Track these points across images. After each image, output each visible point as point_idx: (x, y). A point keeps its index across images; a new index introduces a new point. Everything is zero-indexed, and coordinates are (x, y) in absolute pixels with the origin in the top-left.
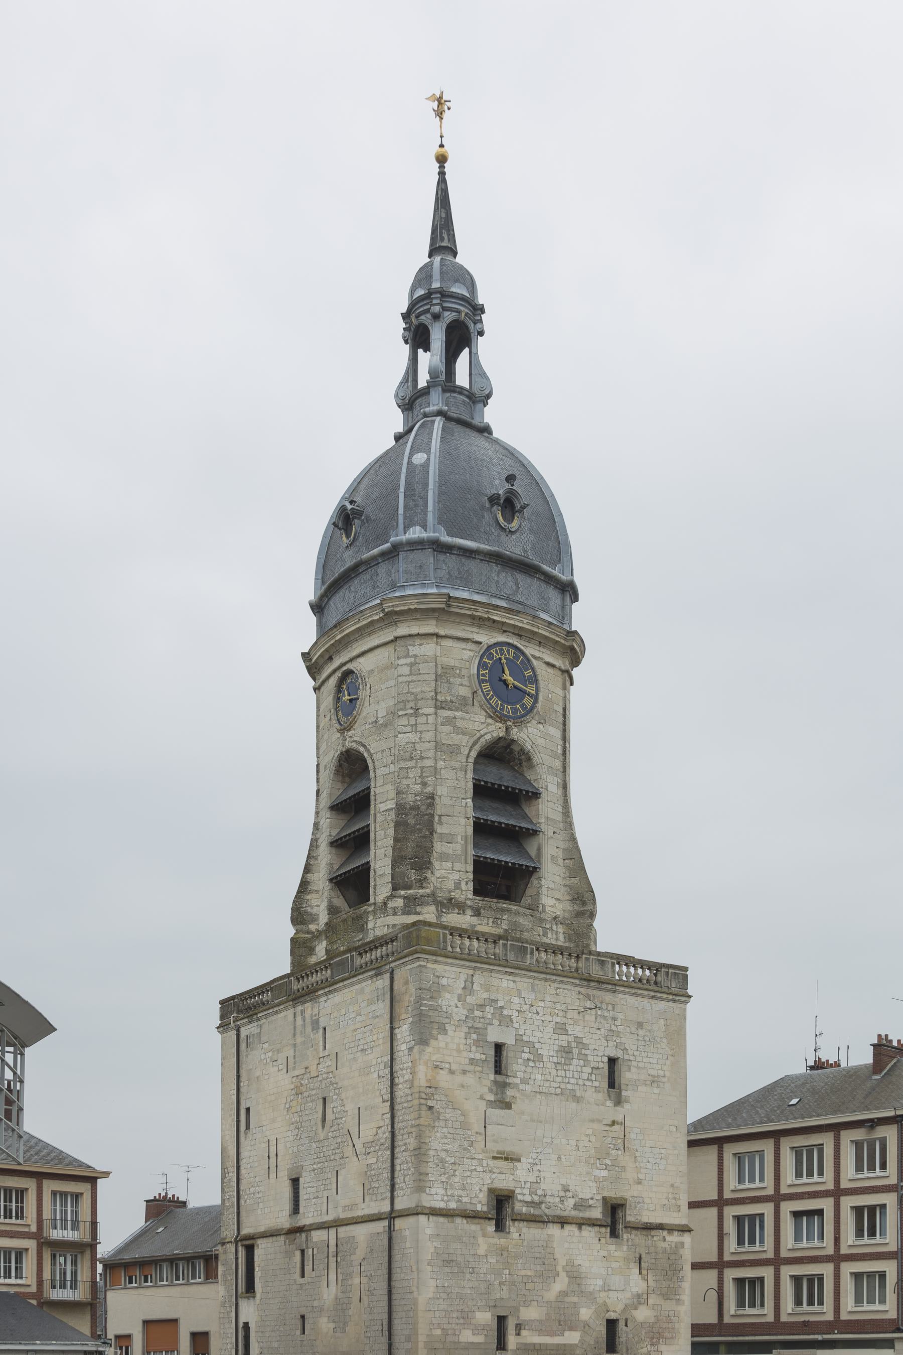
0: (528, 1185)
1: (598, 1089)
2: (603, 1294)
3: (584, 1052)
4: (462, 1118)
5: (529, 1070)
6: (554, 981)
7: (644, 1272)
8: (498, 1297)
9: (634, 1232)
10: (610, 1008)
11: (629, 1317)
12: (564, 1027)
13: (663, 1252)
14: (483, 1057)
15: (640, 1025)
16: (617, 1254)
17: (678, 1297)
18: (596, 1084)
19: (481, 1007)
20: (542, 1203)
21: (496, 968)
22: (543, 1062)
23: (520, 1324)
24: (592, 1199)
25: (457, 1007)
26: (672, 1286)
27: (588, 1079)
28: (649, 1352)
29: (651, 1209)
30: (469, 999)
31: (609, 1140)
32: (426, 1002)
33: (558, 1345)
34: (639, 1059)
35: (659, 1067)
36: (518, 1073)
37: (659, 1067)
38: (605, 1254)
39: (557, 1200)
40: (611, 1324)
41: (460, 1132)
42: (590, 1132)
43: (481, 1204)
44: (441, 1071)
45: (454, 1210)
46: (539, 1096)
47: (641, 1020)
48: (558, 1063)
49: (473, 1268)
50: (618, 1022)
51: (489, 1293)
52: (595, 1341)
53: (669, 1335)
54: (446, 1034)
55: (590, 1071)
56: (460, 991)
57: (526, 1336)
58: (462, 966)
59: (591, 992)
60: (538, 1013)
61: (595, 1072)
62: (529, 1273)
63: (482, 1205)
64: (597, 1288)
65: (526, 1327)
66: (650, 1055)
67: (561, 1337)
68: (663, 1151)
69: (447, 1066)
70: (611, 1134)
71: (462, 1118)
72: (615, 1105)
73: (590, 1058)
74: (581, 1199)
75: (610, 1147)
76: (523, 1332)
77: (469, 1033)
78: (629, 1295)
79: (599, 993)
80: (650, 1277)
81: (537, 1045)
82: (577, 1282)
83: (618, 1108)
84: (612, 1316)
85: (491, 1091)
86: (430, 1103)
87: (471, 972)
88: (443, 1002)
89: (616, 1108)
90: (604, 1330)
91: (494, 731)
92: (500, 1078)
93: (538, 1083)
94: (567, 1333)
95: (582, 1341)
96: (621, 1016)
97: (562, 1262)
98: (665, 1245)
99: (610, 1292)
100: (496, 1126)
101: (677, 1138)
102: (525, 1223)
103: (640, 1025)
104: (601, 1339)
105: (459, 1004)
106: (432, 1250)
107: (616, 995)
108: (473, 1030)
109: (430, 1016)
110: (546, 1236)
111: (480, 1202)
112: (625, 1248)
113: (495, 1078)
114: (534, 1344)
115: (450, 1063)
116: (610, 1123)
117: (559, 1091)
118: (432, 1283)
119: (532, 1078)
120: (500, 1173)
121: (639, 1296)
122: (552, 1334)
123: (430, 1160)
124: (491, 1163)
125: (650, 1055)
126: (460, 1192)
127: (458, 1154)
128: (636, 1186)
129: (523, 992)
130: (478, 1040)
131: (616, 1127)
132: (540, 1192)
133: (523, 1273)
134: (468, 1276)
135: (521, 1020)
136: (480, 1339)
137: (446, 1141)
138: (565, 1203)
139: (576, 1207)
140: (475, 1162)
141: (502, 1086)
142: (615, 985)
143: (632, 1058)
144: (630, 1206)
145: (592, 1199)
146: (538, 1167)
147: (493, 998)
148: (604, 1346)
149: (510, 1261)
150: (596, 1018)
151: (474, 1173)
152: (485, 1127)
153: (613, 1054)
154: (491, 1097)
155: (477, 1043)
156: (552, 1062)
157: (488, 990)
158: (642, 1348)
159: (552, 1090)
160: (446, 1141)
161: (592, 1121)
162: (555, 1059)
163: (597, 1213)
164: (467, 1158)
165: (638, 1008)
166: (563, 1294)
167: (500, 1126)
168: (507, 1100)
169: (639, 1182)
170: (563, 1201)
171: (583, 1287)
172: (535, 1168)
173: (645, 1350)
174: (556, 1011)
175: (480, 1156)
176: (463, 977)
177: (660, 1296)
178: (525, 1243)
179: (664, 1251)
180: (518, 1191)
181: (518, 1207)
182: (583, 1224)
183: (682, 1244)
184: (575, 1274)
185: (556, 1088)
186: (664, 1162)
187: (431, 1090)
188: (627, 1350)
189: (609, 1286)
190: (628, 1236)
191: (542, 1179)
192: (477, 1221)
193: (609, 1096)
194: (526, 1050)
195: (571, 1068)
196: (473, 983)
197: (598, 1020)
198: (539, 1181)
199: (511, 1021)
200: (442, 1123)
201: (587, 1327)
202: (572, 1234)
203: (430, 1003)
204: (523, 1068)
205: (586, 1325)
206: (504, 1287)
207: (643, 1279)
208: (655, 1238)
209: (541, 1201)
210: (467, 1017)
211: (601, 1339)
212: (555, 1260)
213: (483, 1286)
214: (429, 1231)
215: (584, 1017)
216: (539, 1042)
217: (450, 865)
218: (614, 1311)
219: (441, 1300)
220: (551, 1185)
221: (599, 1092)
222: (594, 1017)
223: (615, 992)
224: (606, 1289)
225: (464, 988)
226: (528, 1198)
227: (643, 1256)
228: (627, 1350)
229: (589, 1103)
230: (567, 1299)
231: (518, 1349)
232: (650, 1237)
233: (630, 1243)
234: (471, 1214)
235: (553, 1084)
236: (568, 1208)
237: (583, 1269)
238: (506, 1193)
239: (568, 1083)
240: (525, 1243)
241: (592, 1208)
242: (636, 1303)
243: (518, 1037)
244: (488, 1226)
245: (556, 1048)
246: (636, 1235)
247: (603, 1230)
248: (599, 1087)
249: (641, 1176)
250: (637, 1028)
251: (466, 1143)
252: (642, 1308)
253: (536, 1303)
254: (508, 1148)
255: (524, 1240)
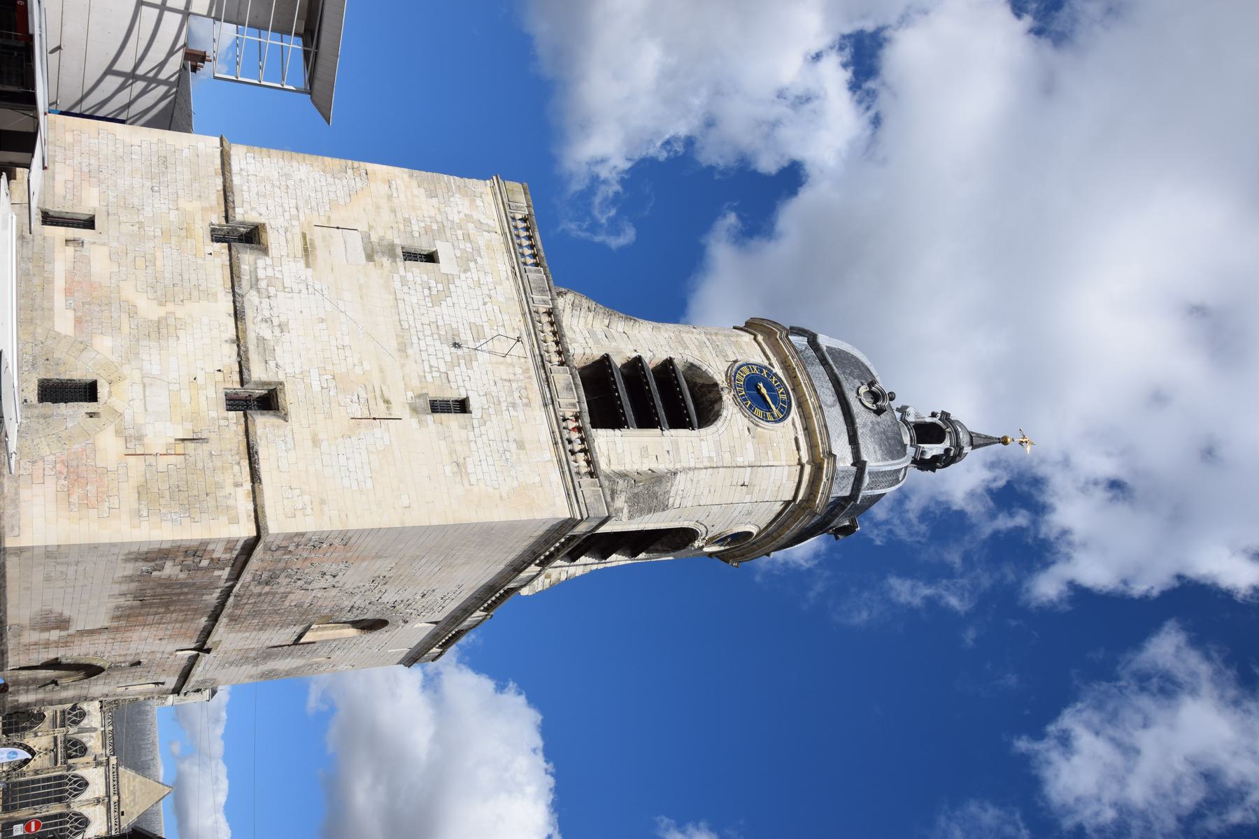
0: (278, 275)
1: (424, 379)
2: (136, 375)
3: (462, 362)
4: (341, 202)
5: (419, 288)
6: (526, 325)
7: (180, 448)
8: (121, 219)
9: (241, 429)
10: (525, 400)
11: (103, 419)
12: (481, 336)
13: (216, 483)
14: (416, 235)
15: (521, 445)
16: (202, 399)
17: (145, 513)
18: (429, 377)
19: (467, 238)
20: (259, 292)
21: (513, 254)
22: (433, 306)
23: (82, 246)
24: (277, 366)
25: (459, 212)
26: (162, 501)
27: (431, 367)
28: (43, 459)
29: (280, 463)
30: (471, 226)
31: (363, 395)
32: (452, 181)
33: (51, 299)
34: (479, 440)
35: (480, 476)
36: (410, 274)
37: (480, 476)
38: (200, 381)
39: (267, 314)
40: (89, 392)
41: (326, 200)
42: (367, 366)
43: (245, 214)
44: (387, 186)
45: (231, 181)
46: (391, 297)
47: (527, 447)
48: (437, 326)
49: (159, 191)
50: (513, 413)
51: (126, 208)
52: (60, 359)
53: (74, 499)
54: (427, 197)
55: (443, 369)
56: (475, 217)
57: (65, 251)
58: (501, 221)
59: (532, 372)
60: (485, 304)
61: (443, 375)
62: (159, 263)
63: (243, 215)
64: (147, 366)
65: (79, 253)
66: (490, 459)
67: (63, 305)
68: (369, 484)
69: (395, 194)
70: (371, 396)
71: (343, 203)
72: (410, 405)
73: (457, 369)
74: (274, 350)
75: (353, 395)
76: (70, 250)
77: (437, 222)
78: (140, 420)
79: (536, 386)
80: (173, 459)
81: (448, 299)
82: (153, 335)
83: (408, 410)
84: (102, 391)
85: (382, 239)
86: (350, 171)
87: (499, 231)
88: (457, 198)
89: (407, 406)
90: (79, 372)
91: (720, 379)
92: (399, 252)
93: (406, 297)
94: (70, 315)
95: (58, 337)
96: (522, 417)
97: (180, 312)
98: (229, 489)
99: (141, 386)
100: (343, 242)
101: (394, 508)
102: (228, 263)
103: (521, 445)
104: (62, 369)
105: (462, 215)
106: (178, 147)
107: (543, 409)
108: (440, 225)
109: (440, 183)
110: (214, 290)
111: (246, 212)
112: (213, 414)
113: (397, 245)
114: (52, 262)
115: (398, 197)
116: (386, 395)
117: (405, 325)
118: (136, 141)
119: (412, 292)
120: (287, 240)
121: (140, 438)
122: (69, 292)
123: (286, 162)
124: (297, 231)
125: (491, 462)
126: (254, 190)
127: (299, 193)
128: (310, 438)
129: (501, 287)
130: (432, 230)
131: (383, 406)
132: (272, 290)
133: (159, 254)
134: (148, 184)
135: (470, 281)
136: (59, 189)
137: (312, 182)
138: (264, 325)
139: (261, 340)
140: (294, 211)
141: (390, 251)
142: (553, 403)
143: (477, 431)
144: (278, 427)
145: (277, 366)
146: (304, 291)
147: (482, 253)
148: (53, 375)
149: (174, 240)
150: (506, 380)
151: (281, 209)
152: (338, 228)
153: (473, 404)
154: (374, 238)
155: (427, 230)
156: (437, 318)
157: (488, 247)
158: (48, 445)
159: (403, 317)
160: (312, 182)
161: (382, 371)
162: (440, 323)
163: (258, 372)
164: (297, 203)
165: (539, 441)
166: (132, 312)
167: (344, 246)
168: (376, 258)
169: (316, 442)
170: (266, 322)
171: (146, 343)
172: (303, 287)
173: (45, 451)
174: (495, 328)
175: (302, 218)
176: (491, 222)
177: (143, 479)
178: (200, 261)
179: (219, 486)
180: (268, 260)
181: (247, 258)
182: (238, 346)
183: (234, 520)
184: (164, 331)
185: (408, 321)
186: (355, 487)
187: (364, 174)
188: (45, 417)
189: (151, 384)
190: (231, 419)
191: (290, 295)
192: (222, 202)
193: (419, 396)
194: (440, 287)
195: (438, 343)
196: (489, 232)
197: (507, 384)
198: (286, 290)
199: (467, 270)
200: (330, 180)
201: (82, 347)
202: (222, 328)
203: (453, 185)
204: (418, 280)
205: (85, 346)
206: (136, 228)
207: (168, 446)
208: (236, 468)
209: (261, 290)
210: (452, 222)
211: (62, 369)
212: (182, 301)
213: (136, 202)
214: (201, 146)
215: (501, 363)
216: (454, 304)
217: (588, 335)
218: (110, 393)
219: (114, 148)
220: (284, 306)
221: (421, 382)
222: (506, 377)
223: (545, 405)
224: (146, 380)
225: (481, 223)
226: (261, 274)
227: (205, 447)
228: (45, 417)
229: (403, 366)
230: (124, 317)
231: (44, 238)
232: (237, 458)
233: (223, 422)
234: (230, 198)
235: (411, 319)
236: (255, 329)
237: (172, 341)
238: (263, 241)
239: (419, 339)
240: (200, 261)
241: (263, 364)
242: (127, 433)
243: (450, 278)
244: (216, 216)
245: (454, 326)
246: (236, 433)
247: (236, 377)
248: (427, 382)
249: (324, 445)
250: (515, 440)
251: (314, 204)
252: (121, 442)
253: (116, 269)
254: (320, 252)
255: (204, 259)
